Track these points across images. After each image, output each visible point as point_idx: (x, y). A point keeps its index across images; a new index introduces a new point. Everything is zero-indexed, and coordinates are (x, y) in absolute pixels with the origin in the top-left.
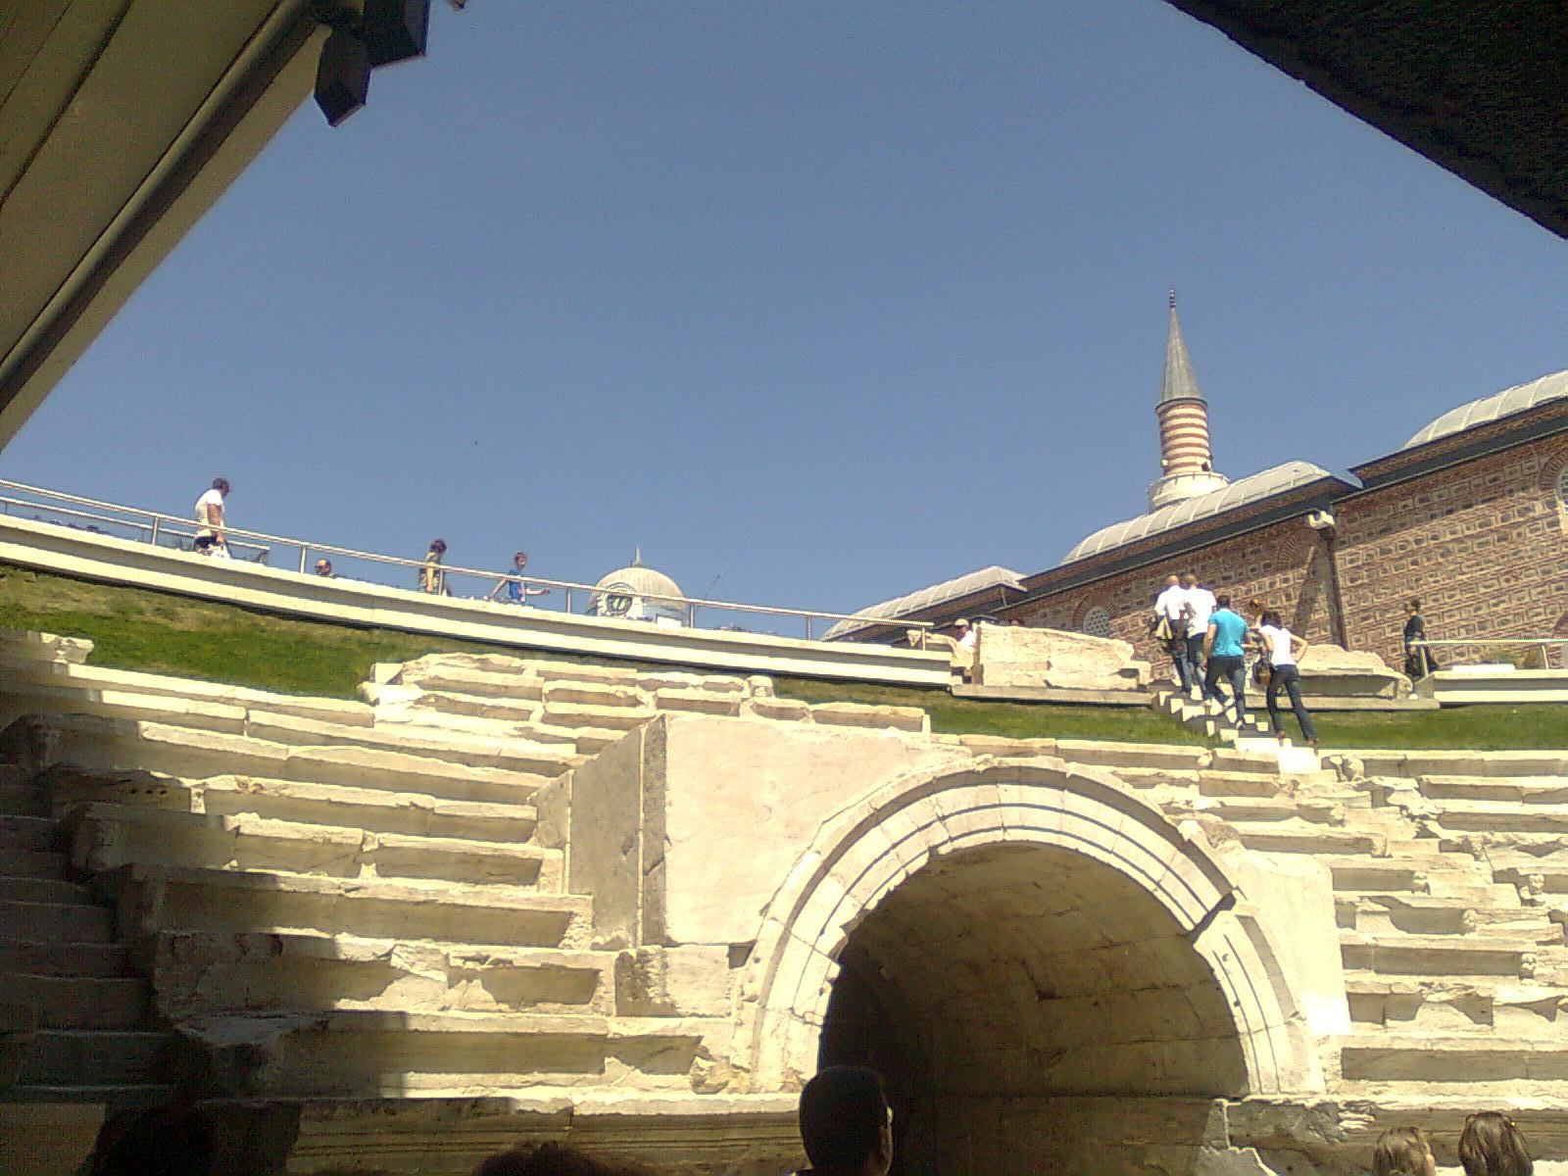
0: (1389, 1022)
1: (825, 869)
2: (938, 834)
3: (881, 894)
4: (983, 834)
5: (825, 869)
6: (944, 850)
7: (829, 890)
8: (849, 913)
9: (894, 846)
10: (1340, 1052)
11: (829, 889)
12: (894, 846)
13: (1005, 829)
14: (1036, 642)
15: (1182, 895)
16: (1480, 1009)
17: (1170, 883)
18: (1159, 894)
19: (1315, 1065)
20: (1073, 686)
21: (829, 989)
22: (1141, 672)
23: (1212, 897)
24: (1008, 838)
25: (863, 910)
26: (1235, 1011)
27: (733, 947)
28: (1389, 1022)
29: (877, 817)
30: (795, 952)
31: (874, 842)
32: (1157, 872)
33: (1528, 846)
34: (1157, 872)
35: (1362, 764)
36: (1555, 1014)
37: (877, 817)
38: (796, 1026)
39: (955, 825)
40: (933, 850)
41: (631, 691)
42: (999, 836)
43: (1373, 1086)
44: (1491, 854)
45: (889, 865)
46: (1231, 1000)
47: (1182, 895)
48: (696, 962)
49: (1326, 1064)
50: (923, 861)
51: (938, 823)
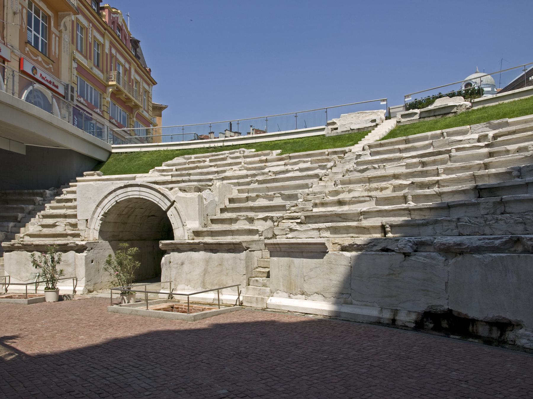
0: (232, 224)
1: (98, 206)
2: (117, 198)
3: (108, 210)
5: (98, 206)
8: (102, 213)
9: (109, 201)
11: (99, 210)
12: (109, 201)
13: (129, 196)
14: (355, 116)
15: (163, 204)
16: (251, 220)
17: (160, 202)
18: (159, 204)
19: (186, 234)
23: (169, 204)
26: (172, 225)
28: (232, 224)
29: (106, 197)
30: (94, 220)
31: (106, 201)
32: (158, 200)
33: (359, 170)
34: (158, 200)
36: (267, 220)
37: (106, 197)
39: (120, 196)
40: (116, 201)
41: (203, 159)
42: (128, 197)
43: (202, 238)
45: (109, 205)
46: (172, 223)
47: (163, 204)
48: (81, 222)
49: (189, 234)
50: (115, 203)
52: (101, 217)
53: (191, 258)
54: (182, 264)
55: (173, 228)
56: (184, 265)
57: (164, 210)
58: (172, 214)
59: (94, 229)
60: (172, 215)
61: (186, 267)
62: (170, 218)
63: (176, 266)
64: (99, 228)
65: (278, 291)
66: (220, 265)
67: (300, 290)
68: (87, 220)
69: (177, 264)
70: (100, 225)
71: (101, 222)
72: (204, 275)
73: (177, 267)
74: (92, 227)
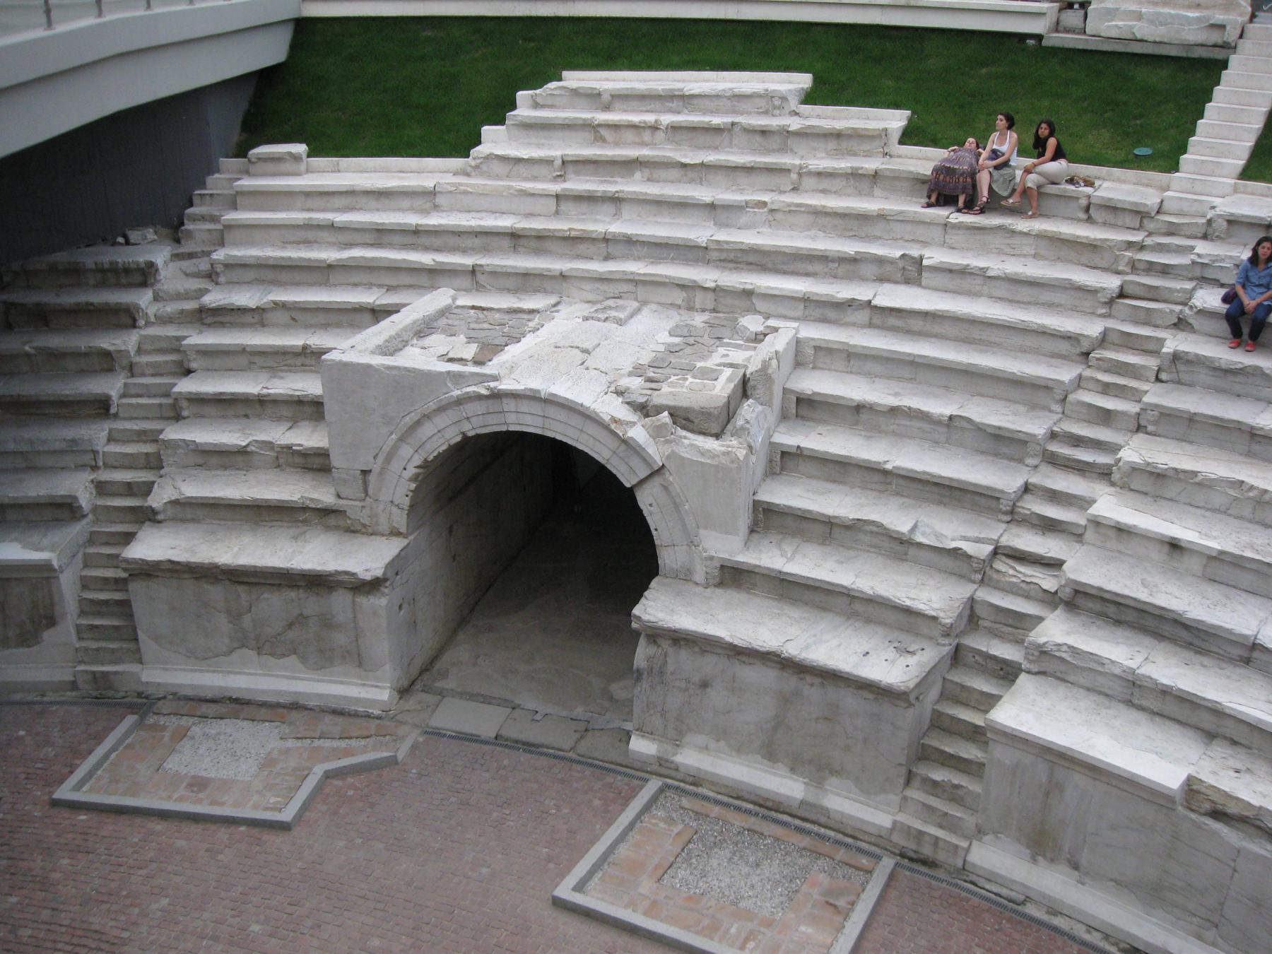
3: (435, 454)
4: (494, 427)
6: (471, 434)
7: (406, 451)
8: (417, 460)
10: (718, 566)
12: (439, 431)
20: (1157, 40)
21: (411, 494)
22: (1228, 28)
24: (510, 429)
25: (425, 460)
26: (654, 533)
27: (362, 471)
35: (1225, 224)
38: (395, 510)
42: (504, 428)
44: (1181, 367)
46: (652, 528)
50: (458, 439)
51: (465, 421)
52: (411, 471)
53: (734, 677)
54: (704, 685)
55: (657, 542)
56: (709, 690)
57: (628, 485)
58: (654, 502)
59: (392, 502)
60: (654, 504)
61: (716, 697)
62: (646, 513)
63: (683, 685)
64: (407, 501)
65: (999, 835)
66: (826, 718)
67: (1068, 856)
68: (365, 473)
69: (688, 681)
70: (410, 494)
71: (413, 486)
72: (775, 729)
73: (687, 690)
74: (385, 496)
